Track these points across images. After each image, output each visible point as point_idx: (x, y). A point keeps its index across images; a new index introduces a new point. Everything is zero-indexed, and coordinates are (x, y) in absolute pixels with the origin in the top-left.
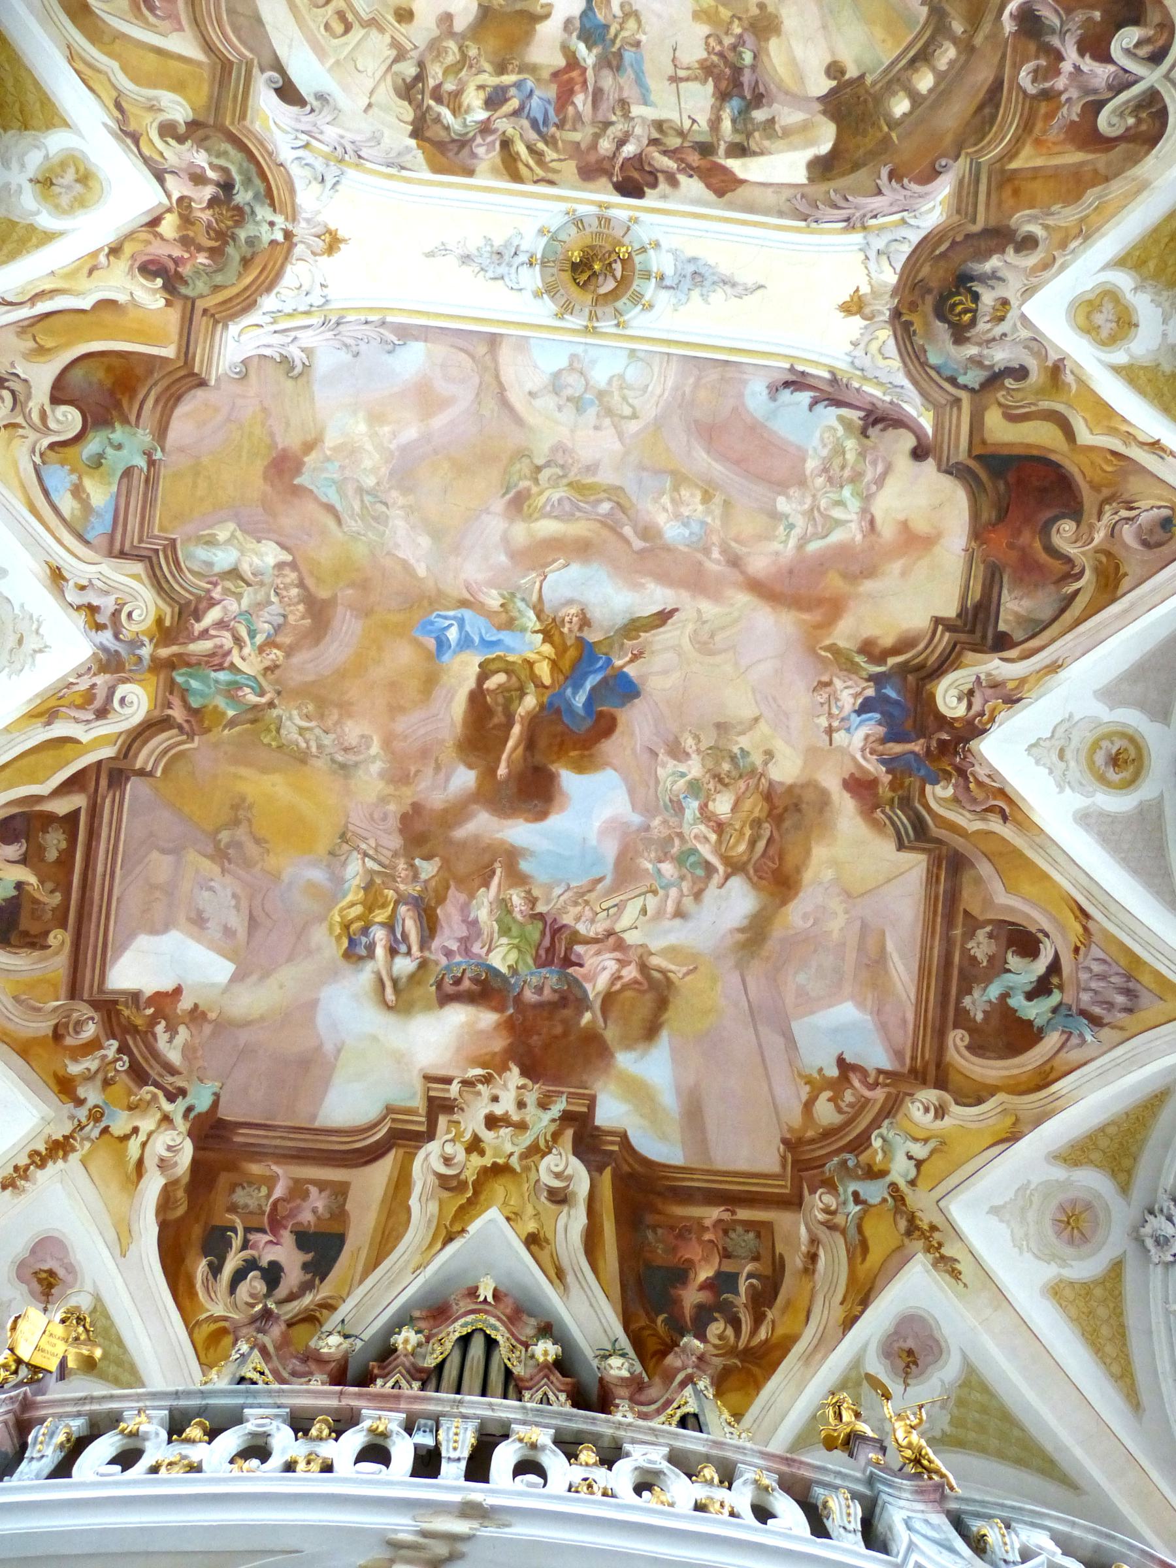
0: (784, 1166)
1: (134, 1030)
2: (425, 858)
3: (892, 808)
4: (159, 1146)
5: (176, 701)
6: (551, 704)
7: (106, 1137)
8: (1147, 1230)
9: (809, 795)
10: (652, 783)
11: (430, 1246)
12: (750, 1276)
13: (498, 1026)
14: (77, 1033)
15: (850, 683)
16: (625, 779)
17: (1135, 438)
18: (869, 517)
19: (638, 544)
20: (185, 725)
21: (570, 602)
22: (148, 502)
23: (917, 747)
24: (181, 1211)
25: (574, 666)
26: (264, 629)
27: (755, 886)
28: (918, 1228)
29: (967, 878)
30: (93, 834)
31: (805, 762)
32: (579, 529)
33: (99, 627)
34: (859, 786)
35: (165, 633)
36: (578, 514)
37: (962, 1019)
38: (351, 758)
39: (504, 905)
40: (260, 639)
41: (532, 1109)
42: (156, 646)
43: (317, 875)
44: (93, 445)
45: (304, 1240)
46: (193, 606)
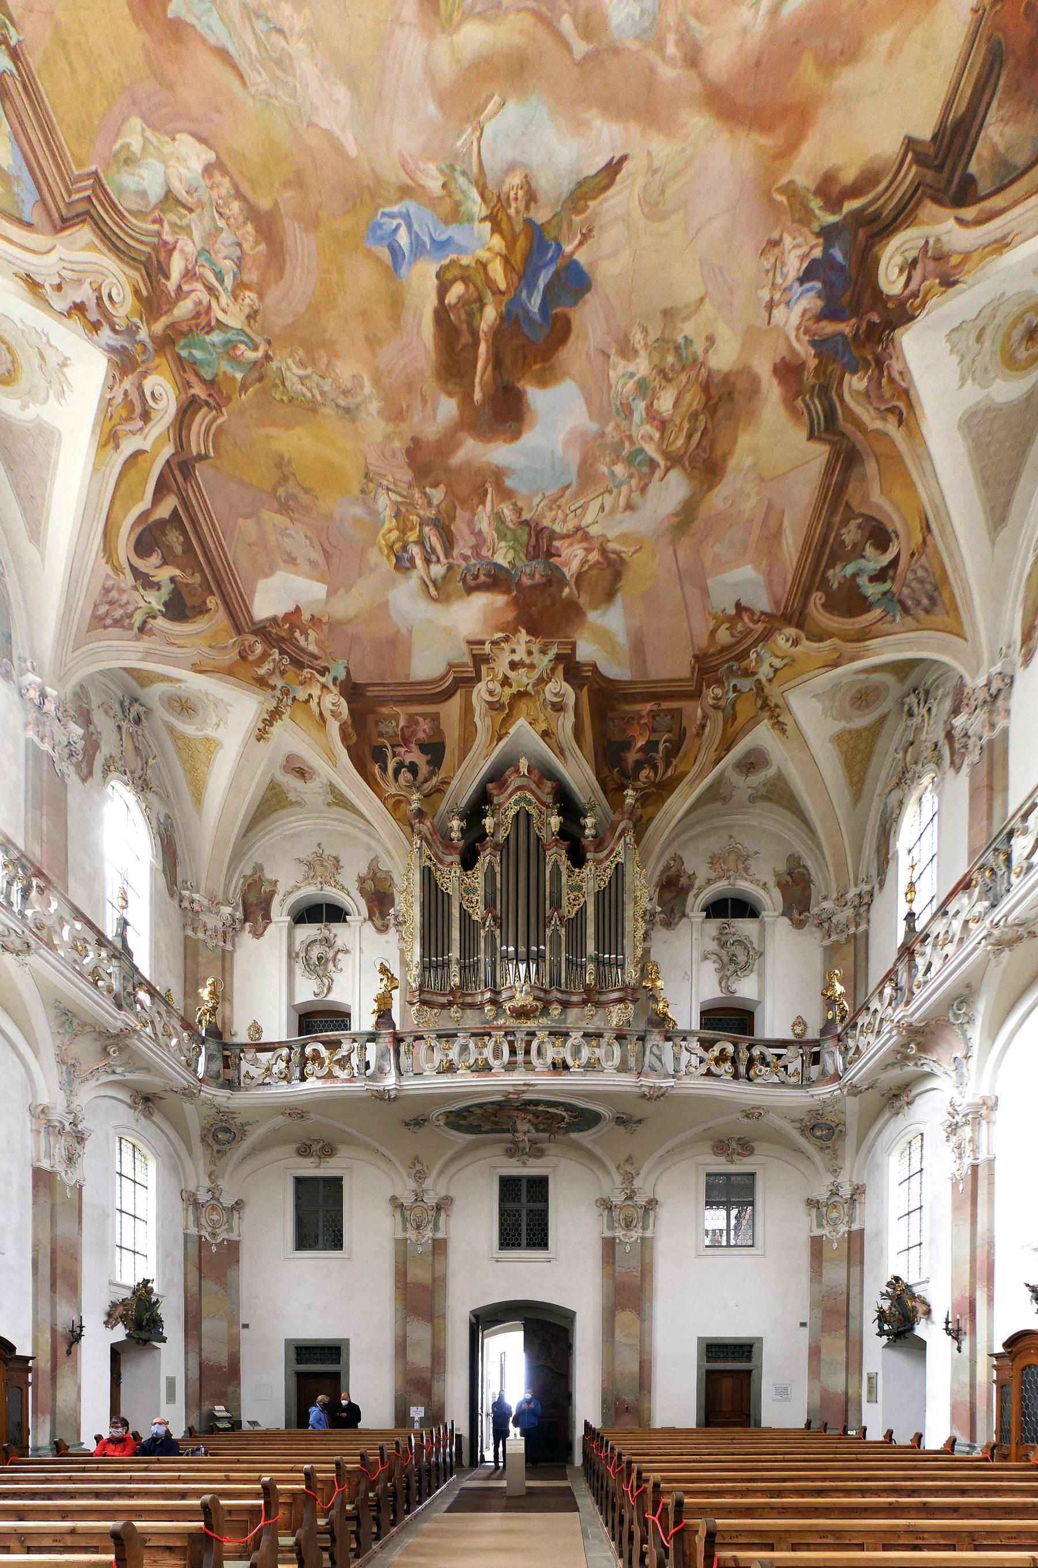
6: (509, 312)
9: (742, 383)
10: (605, 390)
14: (252, 652)
15: (799, 240)
16: (582, 387)
20: (210, 400)
25: (527, 259)
28: (768, 705)
31: (743, 345)
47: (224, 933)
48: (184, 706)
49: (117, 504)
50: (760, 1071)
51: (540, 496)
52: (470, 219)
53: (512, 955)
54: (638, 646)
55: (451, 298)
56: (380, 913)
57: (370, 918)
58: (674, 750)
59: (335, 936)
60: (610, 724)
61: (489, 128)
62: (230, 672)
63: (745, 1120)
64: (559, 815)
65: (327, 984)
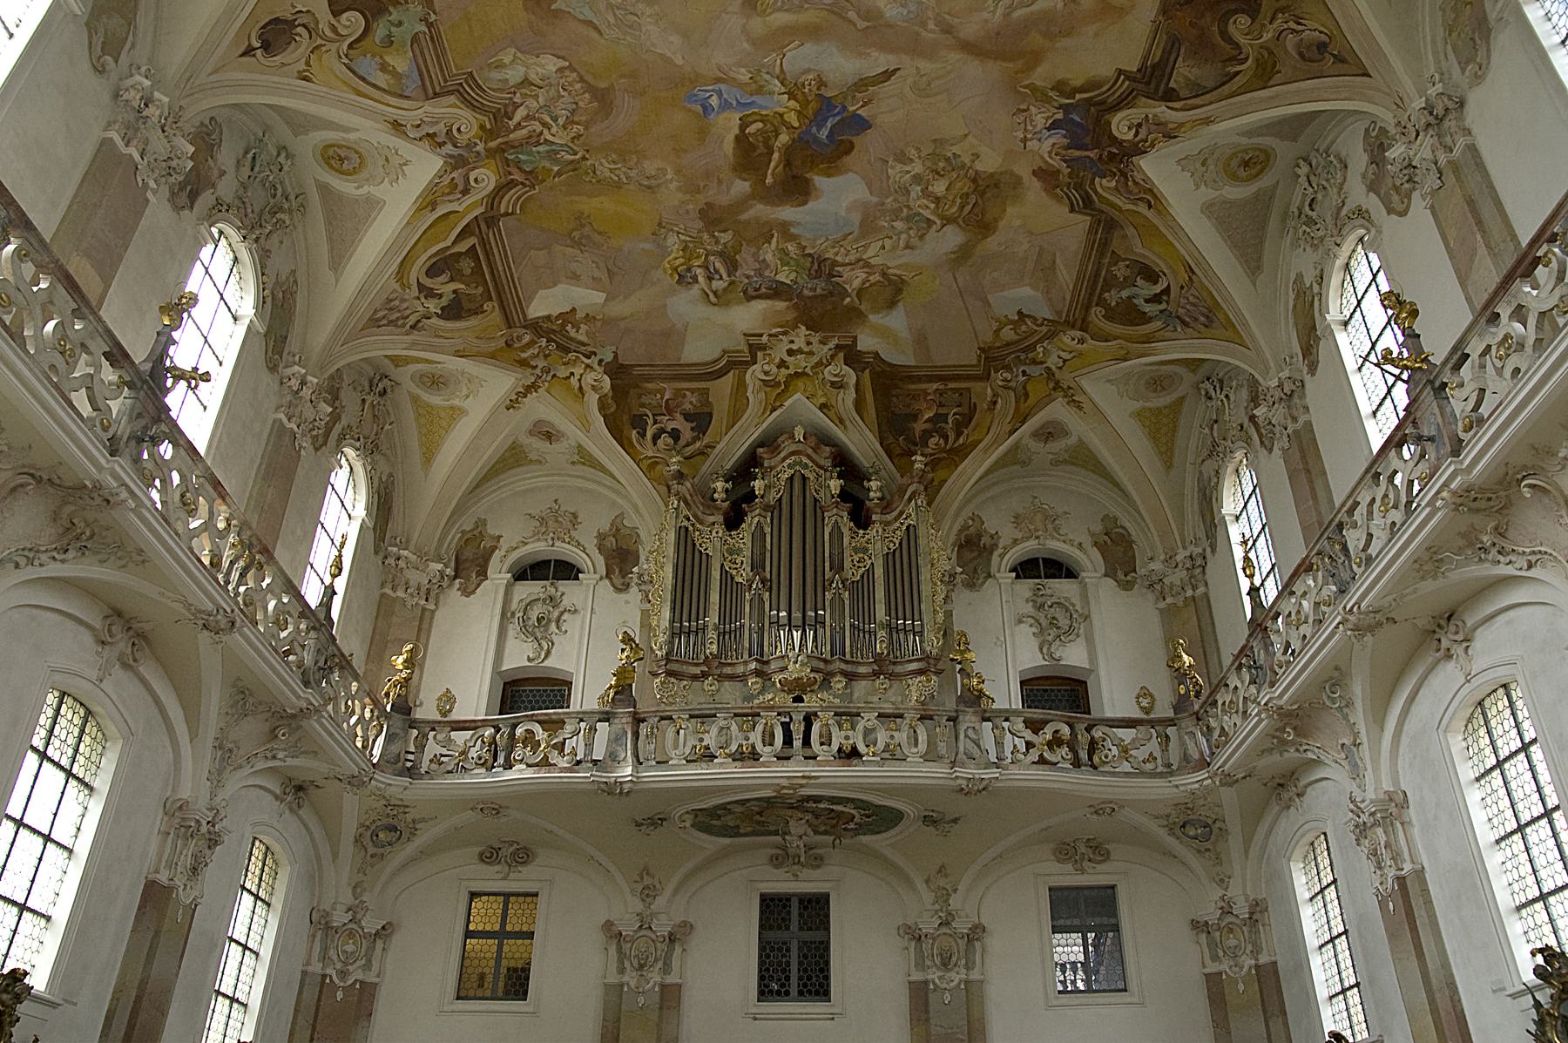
0: (979, 361)
2: (720, 232)
3: (1068, 189)
4: (590, 378)
5: (514, 170)
6: (800, 139)
10: (884, 178)
12: (955, 414)
13: (788, 308)
15: (1043, 110)
19: (861, 24)
20: (527, 182)
21: (808, 71)
22: (440, 54)
24: (613, 410)
25: (816, 114)
27: (964, 230)
32: (809, 17)
33: (441, 145)
34: (1045, 175)
35: (488, 134)
36: (806, 6)
37: (1101, 302)
38: (653, 182)
40: (561, 121)
41: (815, 347)
42: (485, 142)
44: (380, 31)
45: (688, 417)
46: (503, 111)
47: (428, 591)
48: (436, 382)
49: (421, 244)
50: (1106, 757)
51: (823, 239)
53: (784, 621)
54: (921, 340)
56: (621, 571)
57: (608, 576)
59: (563, 594)
60: (894, 399)
62: (493, 356)
63: (1095, 817)
64: (839, 478)
65: (546, 648)
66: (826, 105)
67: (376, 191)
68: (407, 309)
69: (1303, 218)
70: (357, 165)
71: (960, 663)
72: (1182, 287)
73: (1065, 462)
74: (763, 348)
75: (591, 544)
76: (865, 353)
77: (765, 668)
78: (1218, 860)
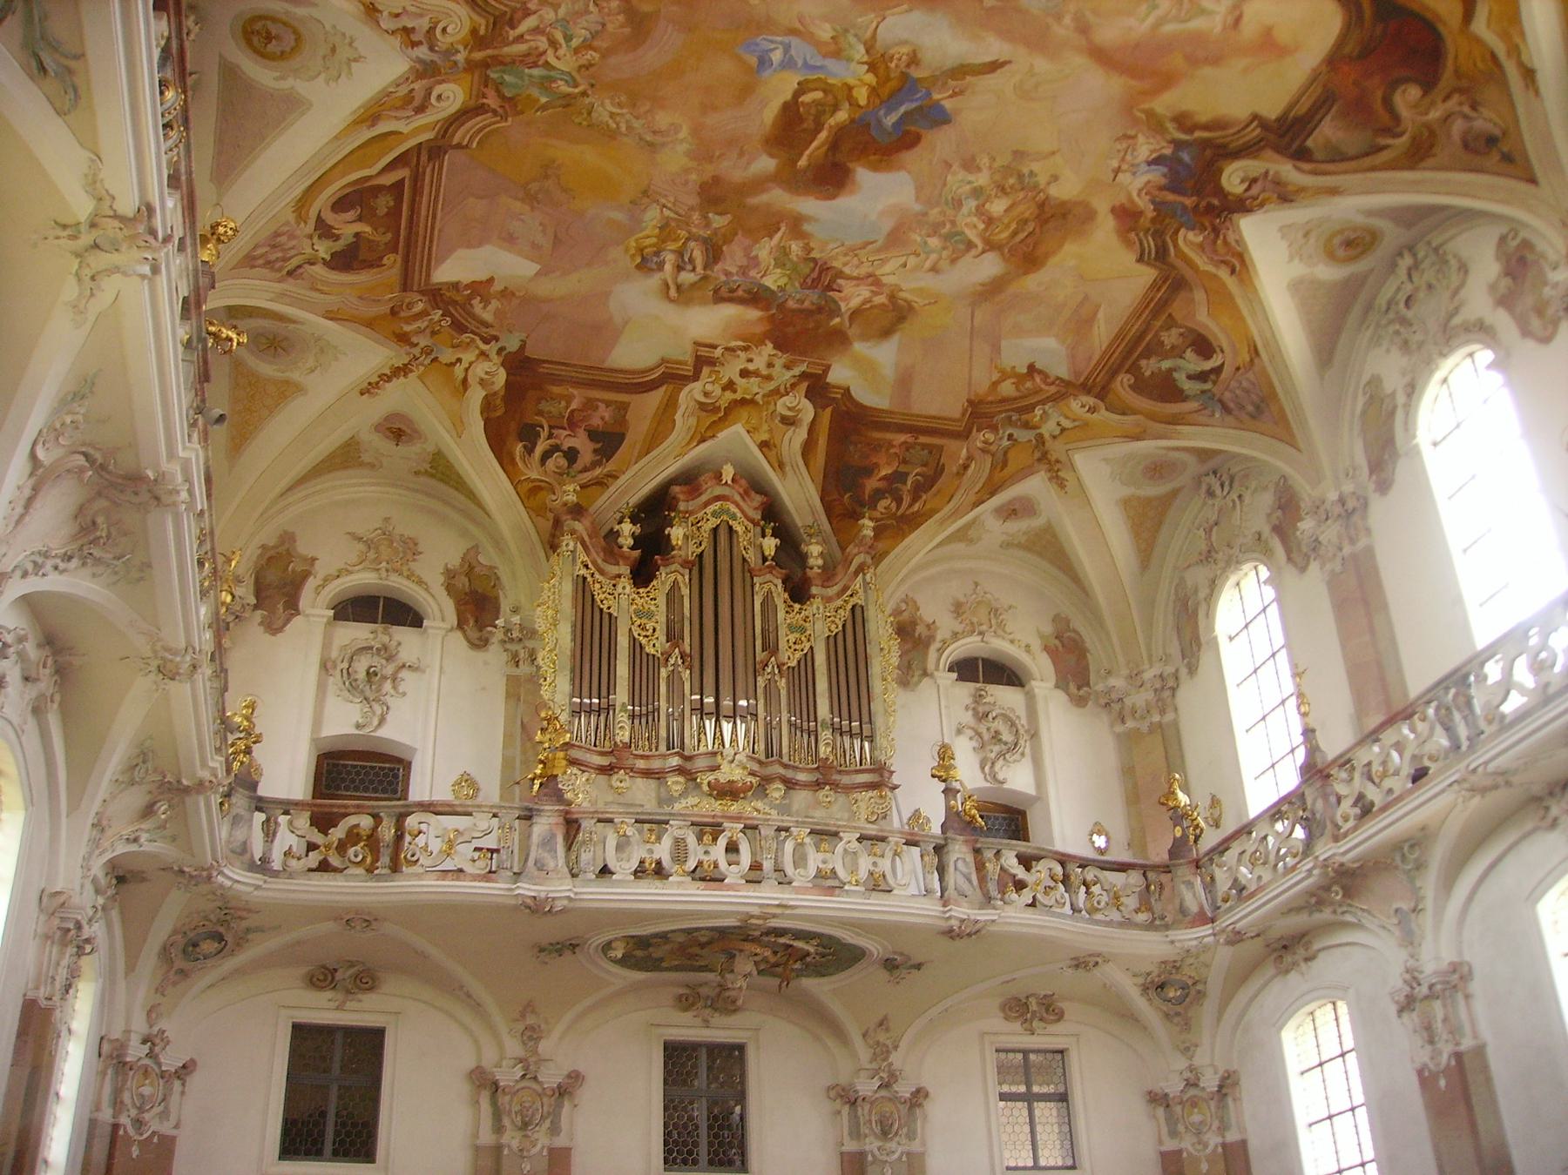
0: (963, 415)
1: (455, 303)
4: (481, 369)
5: (491, 92)
7: (435, 364)
8: (1207, 479)
11: (689, 443)
17: (1519, 55)
18: (1238, 13)
20: (500, 111)
21: (904, 43)
23: (1189, 202)
24: (498, 414)
25: (892, 95)
26: (580, 34)
27: (1005, 260)
29: (1183, 295)
30: (416, 190)
33: (414, 44)
34: (1126, 216)
35: (477, 40)
37: (1134, 370)
38: (659, 139)
39: (784, 251)
43: (618, 216)
45: (593, 435)
46: (508, 16)
52: (849, 60)
54: (905, 381)
55: (807, 98)
58: (926, 484)
61: (890, 20)
62: (370, 324)
66: (907, 86)
67: (301, 87)
68: (293, 248)
69: (1391, 315)
70: (288, 49)
71: (944, 781)
72: (1238, 369)
73: (1019, 546)
74: (712, 362)
75: (436, 581)
76: (834, 387)
77: (688, 765)
78: (1187, 1026)
